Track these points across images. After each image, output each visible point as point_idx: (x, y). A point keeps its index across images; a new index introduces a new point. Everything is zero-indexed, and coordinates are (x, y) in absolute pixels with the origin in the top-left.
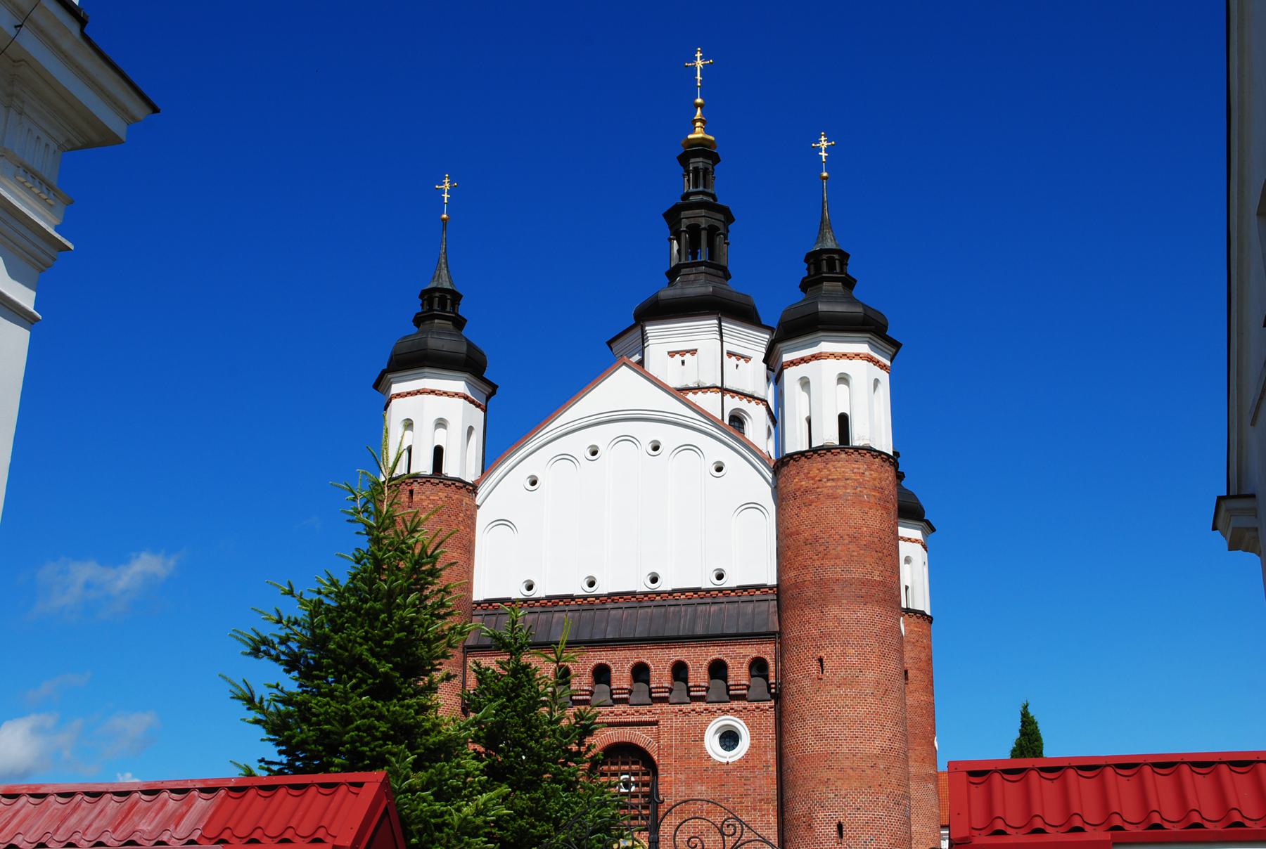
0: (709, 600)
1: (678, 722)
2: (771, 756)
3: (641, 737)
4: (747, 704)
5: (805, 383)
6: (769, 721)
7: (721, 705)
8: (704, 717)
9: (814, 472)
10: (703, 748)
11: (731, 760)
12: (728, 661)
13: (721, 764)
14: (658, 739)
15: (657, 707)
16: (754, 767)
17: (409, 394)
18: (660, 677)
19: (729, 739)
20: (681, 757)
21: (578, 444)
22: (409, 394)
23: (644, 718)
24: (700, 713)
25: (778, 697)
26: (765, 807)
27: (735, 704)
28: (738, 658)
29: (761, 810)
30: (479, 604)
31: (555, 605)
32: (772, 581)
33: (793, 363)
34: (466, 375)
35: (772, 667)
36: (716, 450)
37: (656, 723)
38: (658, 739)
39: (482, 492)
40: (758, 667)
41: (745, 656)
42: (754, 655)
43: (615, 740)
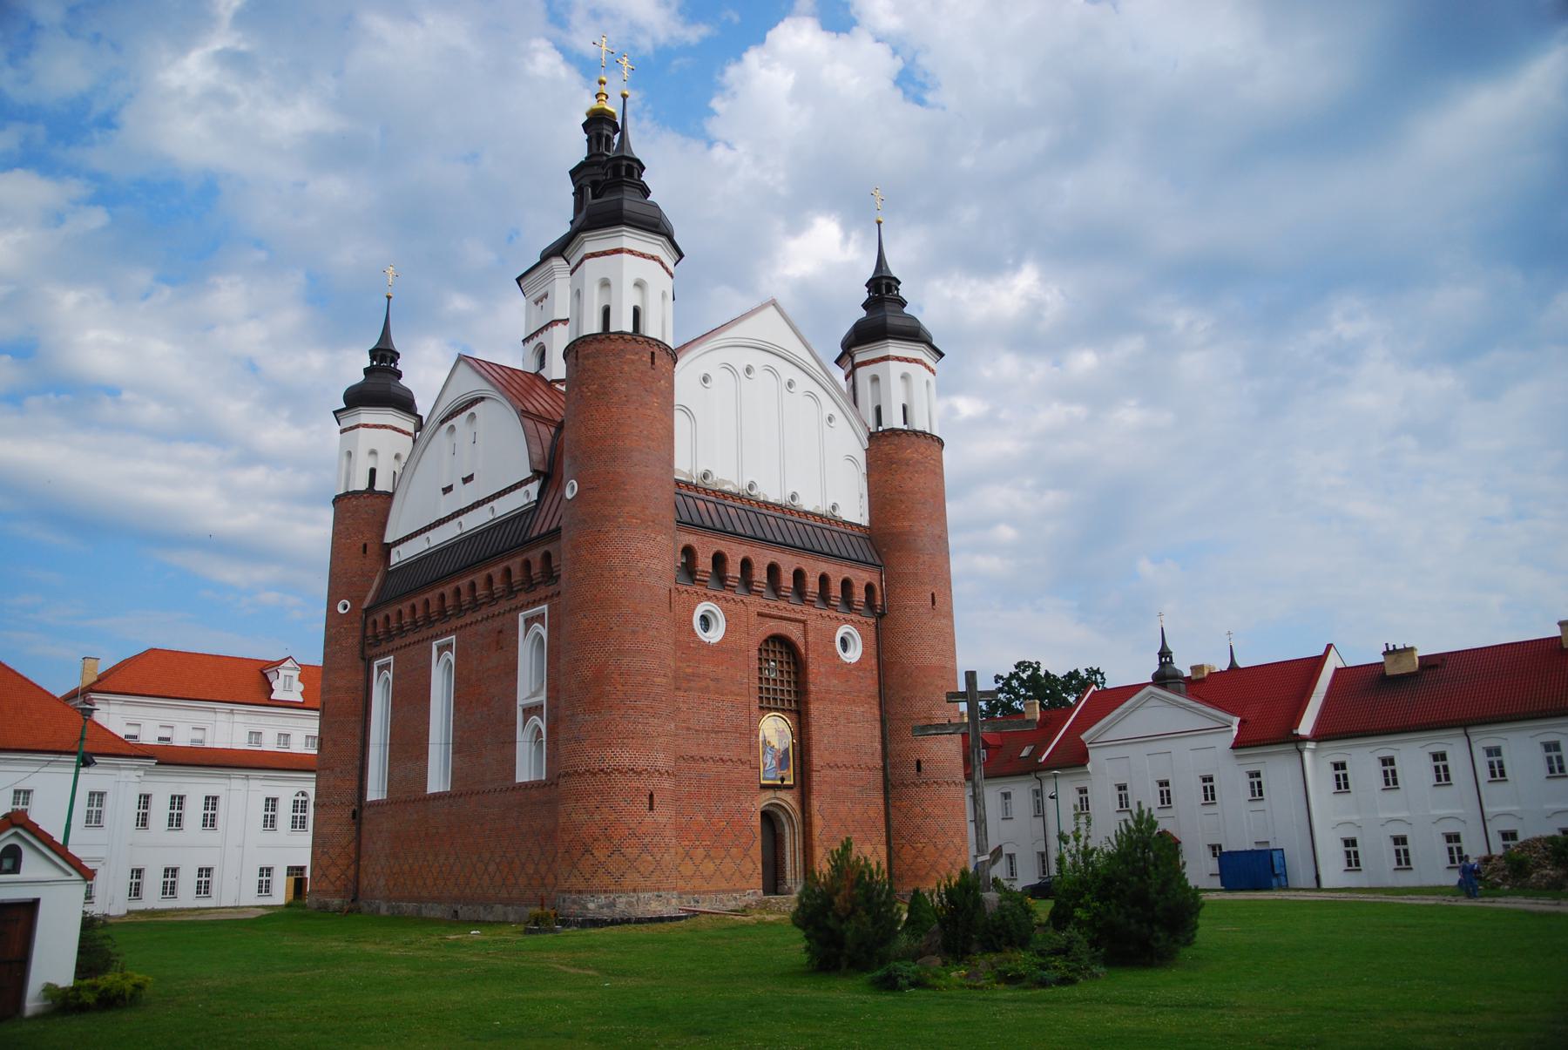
2: (874, 661)
3: (793, 632)
6: (872, 635)
8: (834, 623)
9: (922, 450)
15: (805, 608)
17: (643, 255)
22: (643, 255)
25: (882, 616)
27: (854, 617)
32: (865, 521)
33: (898, 359)
37: (804, 622)
40: (869, 588)
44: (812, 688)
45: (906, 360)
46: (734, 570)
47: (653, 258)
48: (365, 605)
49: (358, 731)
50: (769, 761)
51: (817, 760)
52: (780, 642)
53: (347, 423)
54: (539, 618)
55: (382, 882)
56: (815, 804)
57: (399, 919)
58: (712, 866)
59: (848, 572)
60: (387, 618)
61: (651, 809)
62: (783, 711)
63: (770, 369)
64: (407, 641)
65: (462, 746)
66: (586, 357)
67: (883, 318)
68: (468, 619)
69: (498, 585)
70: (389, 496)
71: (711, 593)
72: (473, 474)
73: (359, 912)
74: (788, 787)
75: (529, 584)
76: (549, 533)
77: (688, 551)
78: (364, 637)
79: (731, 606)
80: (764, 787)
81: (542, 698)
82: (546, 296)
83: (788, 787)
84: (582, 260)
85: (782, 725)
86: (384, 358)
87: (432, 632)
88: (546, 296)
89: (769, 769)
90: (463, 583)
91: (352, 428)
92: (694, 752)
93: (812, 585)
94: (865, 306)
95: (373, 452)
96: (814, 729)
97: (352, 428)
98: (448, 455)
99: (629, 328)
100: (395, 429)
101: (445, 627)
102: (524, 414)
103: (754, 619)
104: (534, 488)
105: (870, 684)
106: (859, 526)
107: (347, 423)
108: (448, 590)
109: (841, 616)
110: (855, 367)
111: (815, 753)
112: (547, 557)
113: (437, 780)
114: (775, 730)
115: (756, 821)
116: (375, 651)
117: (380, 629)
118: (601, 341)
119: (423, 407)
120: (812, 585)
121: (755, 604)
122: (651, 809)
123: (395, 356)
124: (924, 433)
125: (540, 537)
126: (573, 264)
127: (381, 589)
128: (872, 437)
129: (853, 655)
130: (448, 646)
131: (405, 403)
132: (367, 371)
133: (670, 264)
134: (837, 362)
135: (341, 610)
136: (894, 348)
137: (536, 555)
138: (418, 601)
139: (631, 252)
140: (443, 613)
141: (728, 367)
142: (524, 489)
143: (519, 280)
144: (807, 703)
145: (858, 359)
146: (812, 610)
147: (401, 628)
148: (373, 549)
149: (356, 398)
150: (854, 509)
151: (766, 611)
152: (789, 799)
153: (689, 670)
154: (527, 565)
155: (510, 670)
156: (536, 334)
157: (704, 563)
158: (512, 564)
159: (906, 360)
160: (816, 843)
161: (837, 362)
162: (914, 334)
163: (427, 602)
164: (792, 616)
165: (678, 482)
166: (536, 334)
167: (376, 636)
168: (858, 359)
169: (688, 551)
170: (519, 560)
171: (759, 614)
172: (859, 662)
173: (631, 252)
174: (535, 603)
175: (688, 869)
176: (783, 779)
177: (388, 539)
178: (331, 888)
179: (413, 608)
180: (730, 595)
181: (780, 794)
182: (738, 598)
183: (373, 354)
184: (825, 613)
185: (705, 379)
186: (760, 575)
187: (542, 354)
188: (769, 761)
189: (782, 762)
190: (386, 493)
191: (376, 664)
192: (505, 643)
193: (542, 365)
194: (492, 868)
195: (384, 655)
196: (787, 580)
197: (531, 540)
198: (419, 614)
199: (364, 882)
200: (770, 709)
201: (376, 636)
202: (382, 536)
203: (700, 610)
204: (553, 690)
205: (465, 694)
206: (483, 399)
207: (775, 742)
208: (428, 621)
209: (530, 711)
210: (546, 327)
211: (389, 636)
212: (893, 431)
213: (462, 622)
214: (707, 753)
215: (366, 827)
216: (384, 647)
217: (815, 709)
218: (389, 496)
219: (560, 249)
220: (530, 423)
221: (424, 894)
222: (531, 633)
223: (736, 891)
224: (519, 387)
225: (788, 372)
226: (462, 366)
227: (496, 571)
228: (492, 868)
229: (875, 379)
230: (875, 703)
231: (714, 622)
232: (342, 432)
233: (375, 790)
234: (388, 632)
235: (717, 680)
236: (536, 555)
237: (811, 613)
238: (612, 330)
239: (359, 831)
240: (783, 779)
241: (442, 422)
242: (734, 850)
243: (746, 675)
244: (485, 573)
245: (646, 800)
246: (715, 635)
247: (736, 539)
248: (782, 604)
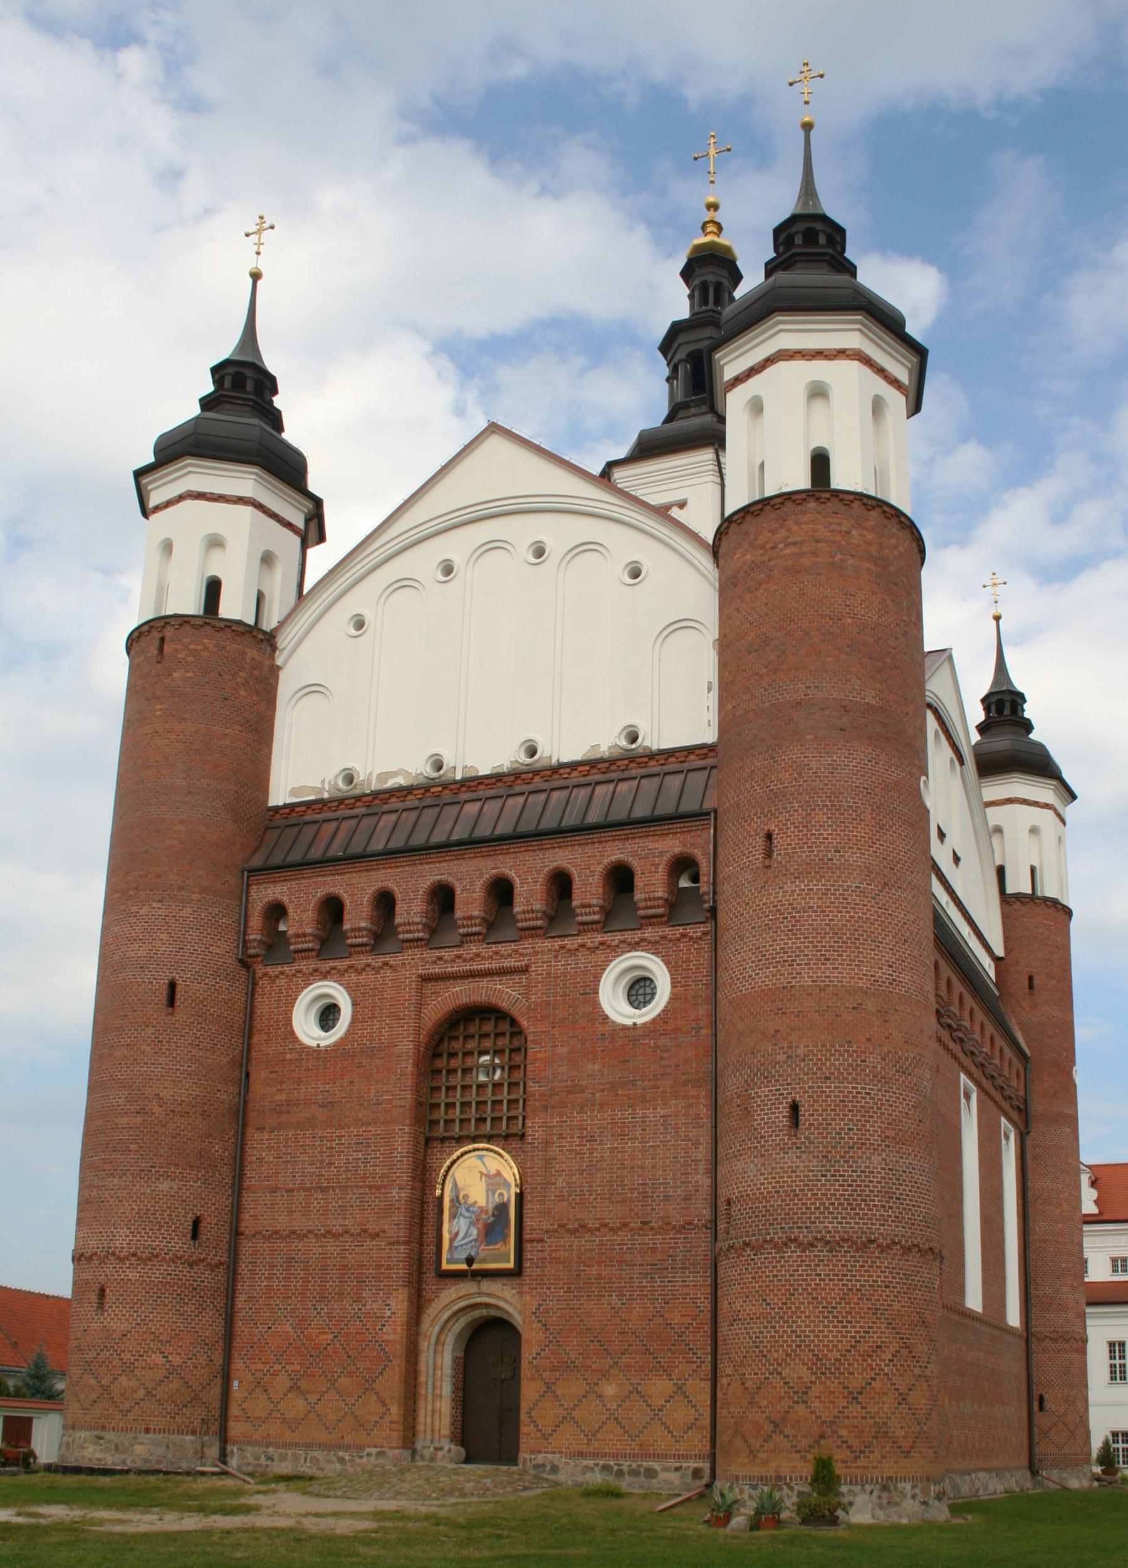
0: (614, 775)
1: (560, 966)
3: (503, 993)
4: (667, 931)
7: (627, 936)
8: (600, 956)
10: (596, 1005)
11: (640, 1021)
12: (635, 864)
13: (625, 1028)
14: (526, 995)
15: (526, 946)
16: (677, 1030)
18: (530, 896)
19: (639, 989)
20: (563, 1020)
21: (422, 563)
23: (507, 963)
24: (593, 950)
26: (693, 1092)
27: (648, 933)
28: (650, 859)
29: (686, 1097)
30: (276, 809)
31: (385, 802)
34: (255, 470)
35: (705, 868)
36: (625, 544)
37: (525, 970)
38: (526, 995)
39: (284, 641)
41: (661, 854)
42: (677, 850)
43: (465, 1000)
44: (532, 1087)
58: (301, 1405)
59: (615, 852)
79: (367, 978)
92: (283, 1223)
109: (614, 938)
141: (403, 584)
151: (436, 970)
153: (281, 1097)
171: (426, 979)
176: (470, 1261)
180: (362, 960)
185: (360, 624)
217: (535, 1128)
223: (347, 1448)
225: (522, 532)
231: (314, 1014)
235: (331, 1104)
242: (345, 1381)
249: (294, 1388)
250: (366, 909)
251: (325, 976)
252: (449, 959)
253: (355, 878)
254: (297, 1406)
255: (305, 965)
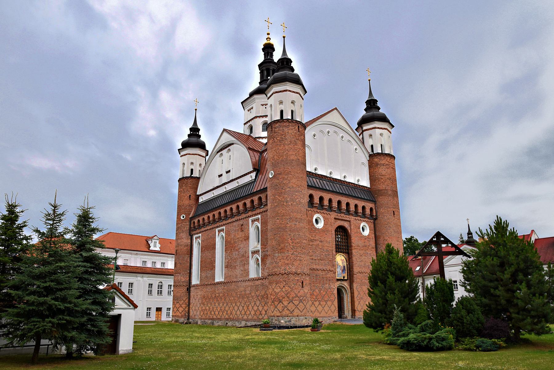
3: (346, 225)
5: (381, 135)
6: (373, 226)
8: (360, 222)
15: (350, 216)
17: (294, 92)
22: (294, 92)
25: (376, 219)
27: (366, 219)
33: (378, 128)
37: (349, 221)
40: (371, 209)
45: (381, 128)
46: (326, 203)
47: (297, 93)
48: (190, 216)
49: (189, 260)
50: (339, 270)
51: (356, 269)
52: (341, 230)
53: (182, 153)
54: (257, 220)
55: (198, 313)
56: (355, 285)
57: (204, 325)
60: (199, 221)
61: (302, 287)
62: (343, 253)
63: (335, 132)
64: (206, 229)
65: (228, 266)
66: (275, 128)
67: (373, 114)
68: (230, 221)
69: (241, 208)
70: (198, 178)
71: (319, 211)
72: (230, 169)
73: (190, 323)
74: (346, 280)
75: (253, 208)
76: (260, 190)
77: (311, 196)
78: (190, 227)
79: (325, 215)
80: (338, 280)
81: (259, 247)
82: (252, 108)
83: (346, 280)
84: (272, 94)
85: (343, 258)
86: (195, 131)
87: (215, 225)
88: (252, 108)
89: (340, 274)
90: (228, 208)
91: (185, 155)
92: (315, 267)
93: (352, 208)
94: (365, 110)
95: (192, 163)
96: (354, 259)
97: (185, 155)
98: (220, 165)
99: (290, 117)
100: (199, 155)
101: (221, 224)
102: (249, 149)
103: (333, 220)
104: (253, 175)
105: (372, 243)
106: (367, 187)
107: (183, 153)
108: (222, 211)
110: (363, 131)
111: (355, 268)
112: (260, 199)
113: (219, 278)
114: (340, 259)
115: (336, 292)
116: (194, 232)
117: (196, 224)
118: (280, 122)
119: (209, 147)
120: (352, 208)
121: (334, 215)
122: (302, 287)
123: (198, 130)
124: (389, 154)
125: (257, 191)
126: (268, 96)
127: (195, 212)
128: (370, 156)
129: (366, 233)
130: (222, 230)
131: (202, 146)
132: (189, 136)
133: (302, 95)
134: (356, 130)
135: (182, 218)
136: (377, 124)
137: (256, 198)
138: (211, 215)
139: (290, 91)
140: (220, 218)
141: (322, 131)
142: (250, 175)
143: (242, 103)
144: (351, 250)
145: (364, 128)
146: (353, 217)
147: (204, 224)
148: (193, 197)
149: (185, 145)
150: (365, 182)
152: (346, 284)
154: (252, 202)
155: (247, 238)
156: (249, 121)
157: (316, 200)
158: (242, 202)
159: (381, 128)
160: (356, 300)
161: (356, 130)
162: (383, 119)
163: (214, 215)
164: (346, 219)
165: (307, 171)
166: (249, 121)
167: (194, 227)
168: (364, 128)
169: (311, 196)
170: (249, 200)
171: (335, 219)
172: (369, 235)
173: (290, 91)
174: (255, 215)
175: (313, 309)
177: (198, 194)
178: (180, 315)
179: (209, 217)
180: (325, 212)
181: (342, 282)
182: (328, 212)
183: (191, 129)
184: (357, 218)
186: (335, 205)
187: (251, 128)
188: (339, 270)
189: (343, 271)
190: (197, 177)
191: (194, 237)
192: (243, 228)
193: (251, 132)
194: (241, 308)
195: (198, 233)
196: (344, 206)
197: (253, 193)
198: (211, 219)
199: (191, 314)
200: (339, 252)
201: (194, 227)
202: (196, 192)
203: (315, 217)
204: (264, 245)
205: (229, 246)
206: (233, 144)
207: (341, 264)
208: (214, 221)
209: (254, 253)
210: (252, 119)
211: (199, 227)
212: (378, 154)
213: (227, 222)
214: (318, 267)
215: (192, 294)
216: (198, 231)
217: (354, 252)
218: (198, 178)
219: (258, 91)
220: (250, 151)
221: (215, 317)
222: (254, 225)
223: (329, 317)
224: (247, 140)
226: (225, 134)
227: (241, 204)
228: (241, 308)
229: (371, 136)
230: (374, 250)
232: (181, 156)
233: (195, 281)
234: (199, 225)
236: (256, 198)
237: (352, 218)
238: (284, 118)
239: (189, 295)
240: (344, 277)
241: (218, 152)
243: (331, 239)
244: (236, 204)
245: (301, 284)
246: (321, 225)
247: (327, 192)
248: (342, 215)
249: (320, 304)
250: (337, 204)
251: (318, 213)
252: (340, 216)
253: (327, 194)
254: (320, 308)
255: (315, 210)
